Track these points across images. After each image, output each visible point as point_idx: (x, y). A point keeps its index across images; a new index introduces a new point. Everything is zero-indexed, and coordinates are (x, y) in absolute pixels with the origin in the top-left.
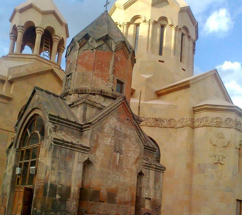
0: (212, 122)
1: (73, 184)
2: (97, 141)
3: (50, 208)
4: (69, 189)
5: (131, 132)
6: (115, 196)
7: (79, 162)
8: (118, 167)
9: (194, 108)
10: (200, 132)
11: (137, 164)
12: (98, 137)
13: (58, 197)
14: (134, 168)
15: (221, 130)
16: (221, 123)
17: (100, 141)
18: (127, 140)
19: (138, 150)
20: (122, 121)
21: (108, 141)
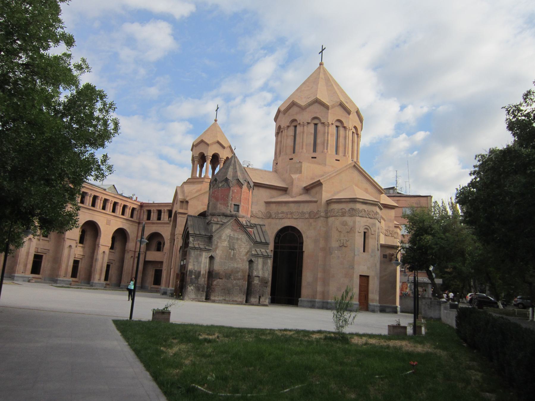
0: (338, 212)
1: (202, 270)
2: (217, 245)
3: (189, 282)
4: (200, 272)
5: (243, 237)
6: (230, 275)
7: (206, 258)
8: (233, 259)
9: (327, 201)
10: (331, 220)
11: (248, 256)
12: (217, 242)
13: (193, 276)
14: (245, 258)
15: (345, 218)
16: (345, 213)
17: (219, 244)
18: (239, 242)
19: (248, 247)
20: (235, 231)
21: (226, 244)
